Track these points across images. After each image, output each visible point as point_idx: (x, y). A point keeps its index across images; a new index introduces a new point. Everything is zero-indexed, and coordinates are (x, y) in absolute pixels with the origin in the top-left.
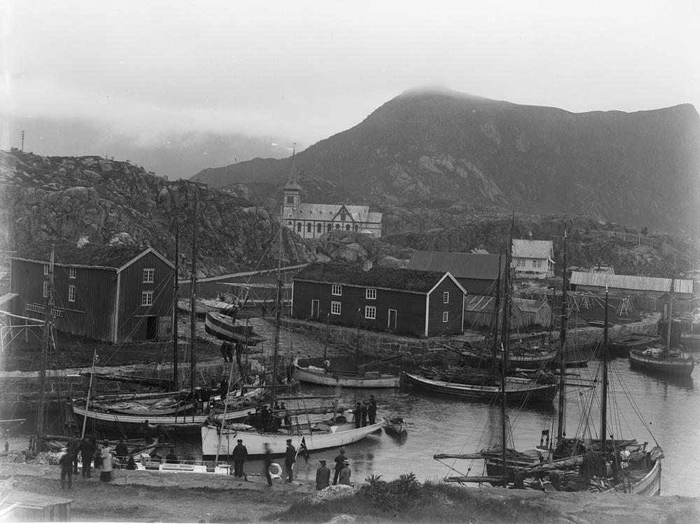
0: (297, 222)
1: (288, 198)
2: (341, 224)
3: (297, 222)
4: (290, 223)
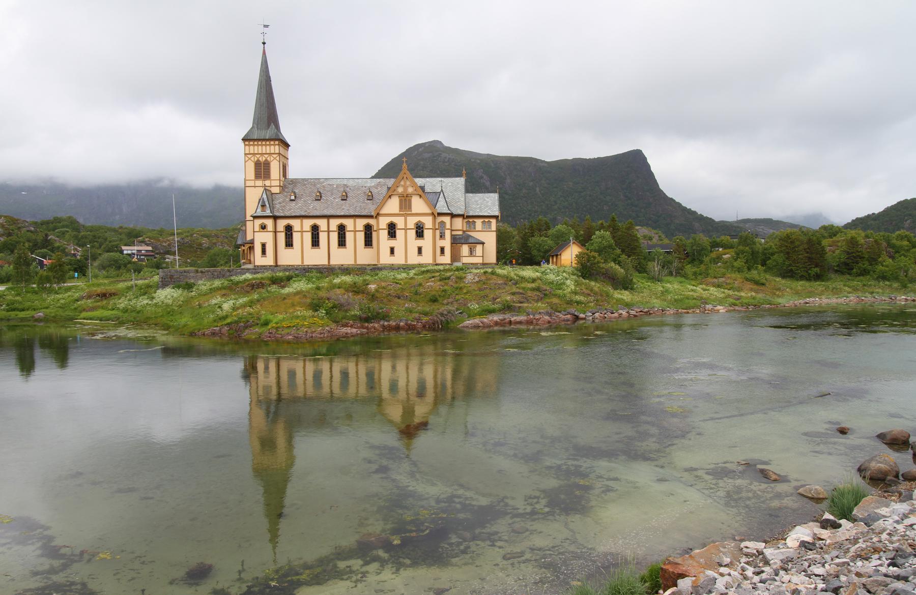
0: (282, 224)
1: (258, 164)
2: (399, 222)
3: (282, 224)
4: (263, 227)
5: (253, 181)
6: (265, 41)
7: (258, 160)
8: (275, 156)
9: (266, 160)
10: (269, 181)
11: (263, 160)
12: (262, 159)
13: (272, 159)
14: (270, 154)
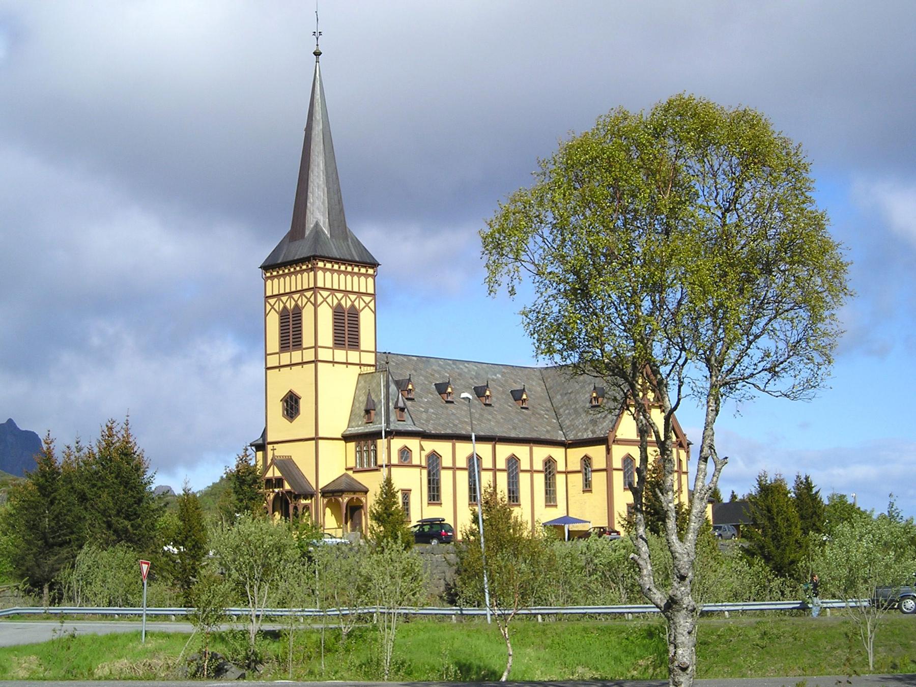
1: (338, 312)
5: (331, 350)
6: (321, 50)
7: (339, 305)
8: (367, 299)
9: (353, 306)
10: (358, 353)
11: (348, 306)
12: (346, 303)
13: (362, 305)
14: (359, 294)
